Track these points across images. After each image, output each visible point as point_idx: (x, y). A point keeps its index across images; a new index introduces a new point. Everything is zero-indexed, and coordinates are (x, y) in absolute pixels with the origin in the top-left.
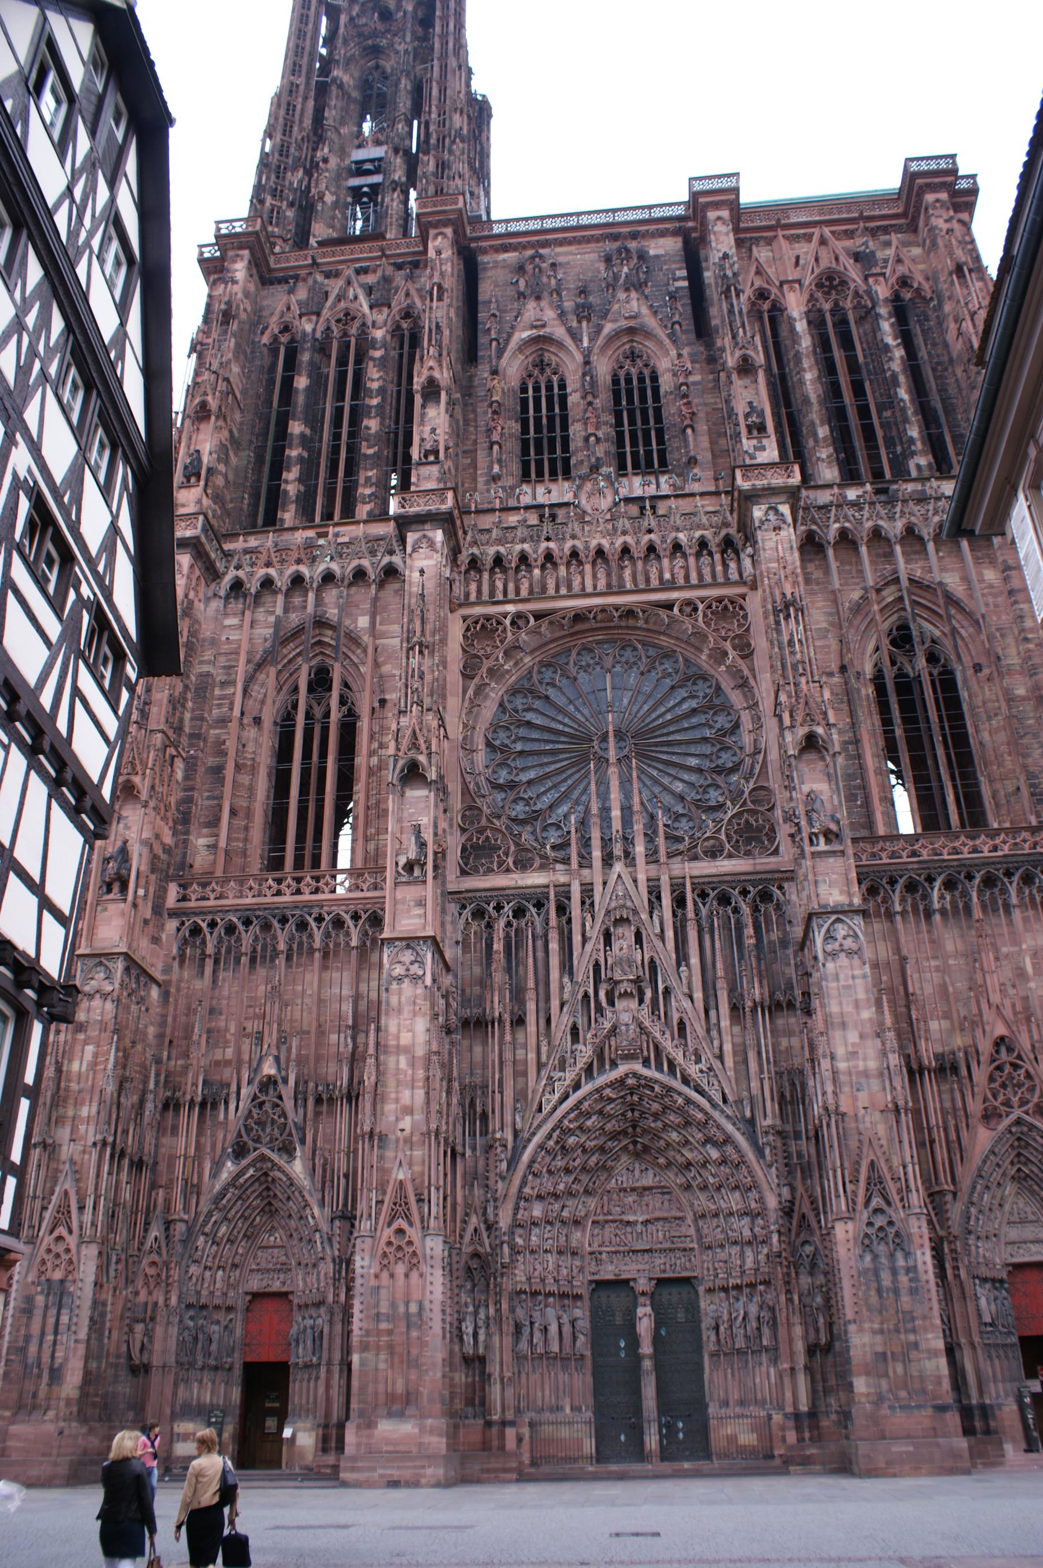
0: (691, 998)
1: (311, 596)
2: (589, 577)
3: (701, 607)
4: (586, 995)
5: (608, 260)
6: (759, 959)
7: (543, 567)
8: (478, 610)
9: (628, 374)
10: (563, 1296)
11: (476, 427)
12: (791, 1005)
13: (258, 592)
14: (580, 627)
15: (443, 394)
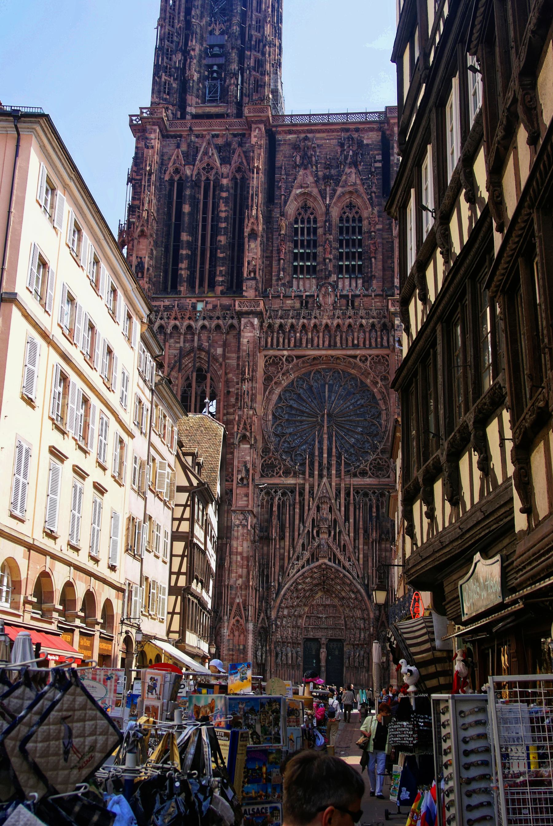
0: (349, 535)
1: (196, 338)
2: (321, 338)
3: (369, 359)
4: (308, 531)
5: (342, 145)
6: (376, 522)
7: (301, 332)
8: (271, 352)
9: (348, 217)
10: (293, 643)
11: (272, 242)
12: (387, 540)
13: (171, 333)
14: (316, 362)
15: (259, 239)
